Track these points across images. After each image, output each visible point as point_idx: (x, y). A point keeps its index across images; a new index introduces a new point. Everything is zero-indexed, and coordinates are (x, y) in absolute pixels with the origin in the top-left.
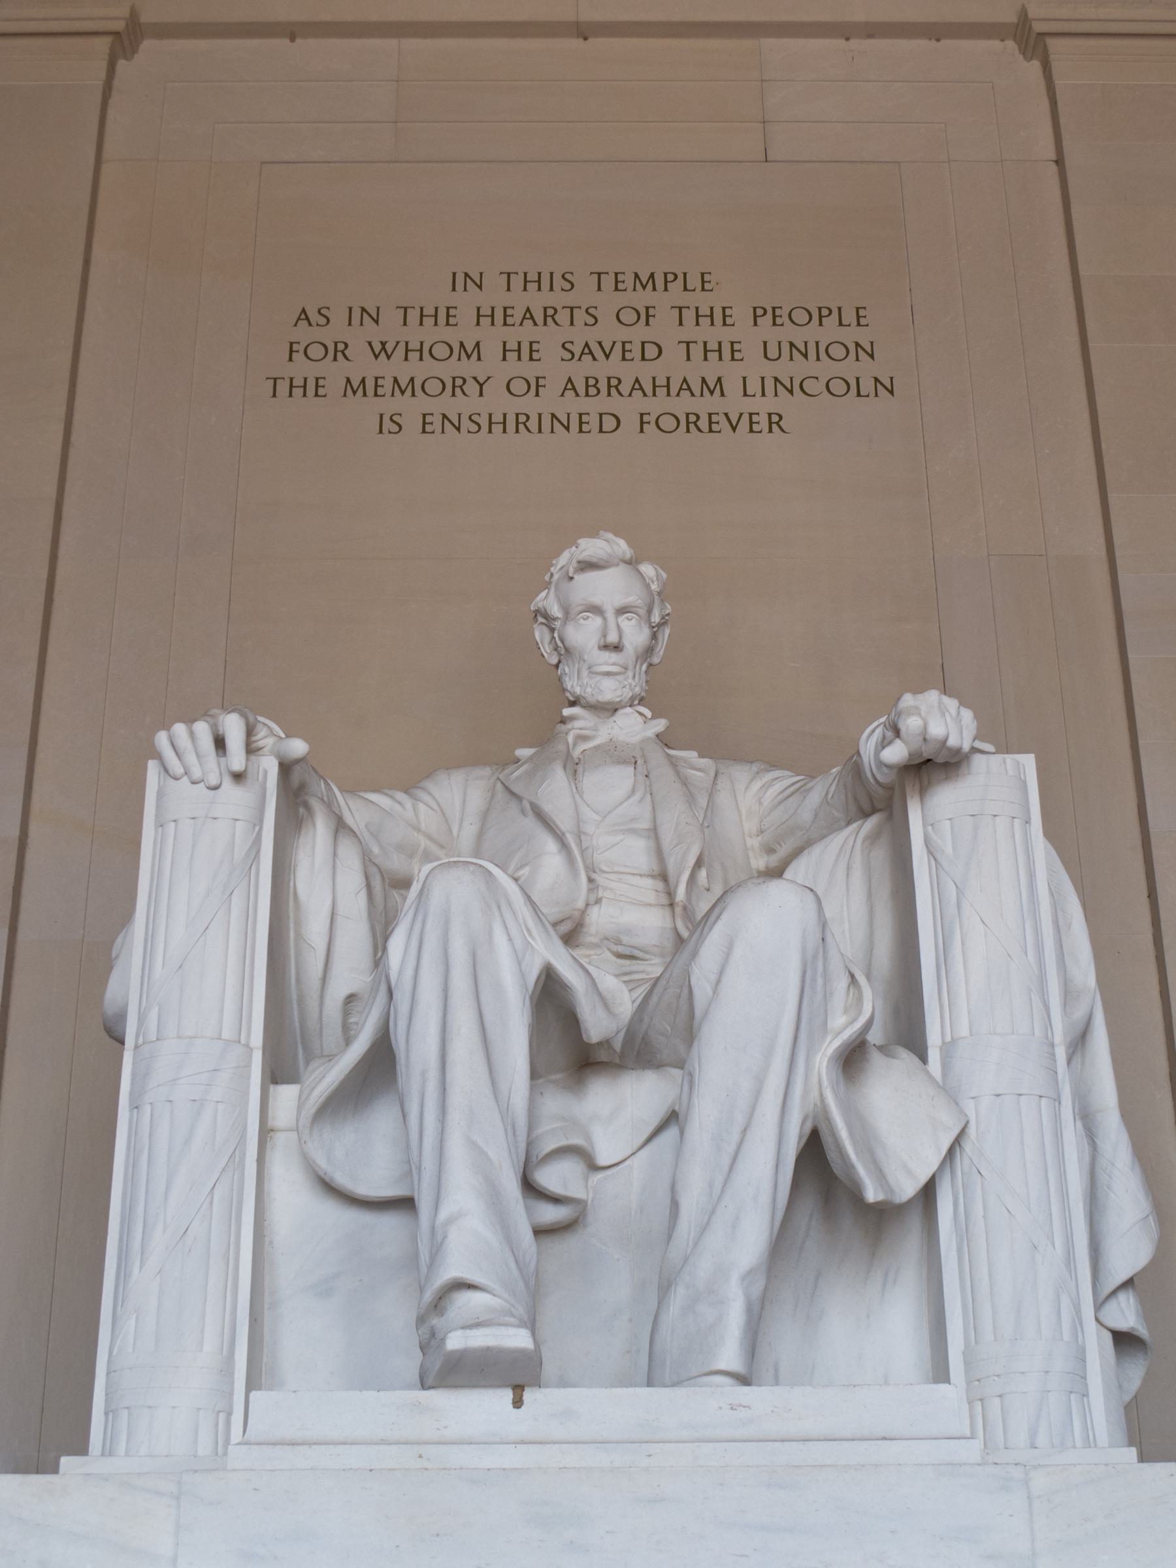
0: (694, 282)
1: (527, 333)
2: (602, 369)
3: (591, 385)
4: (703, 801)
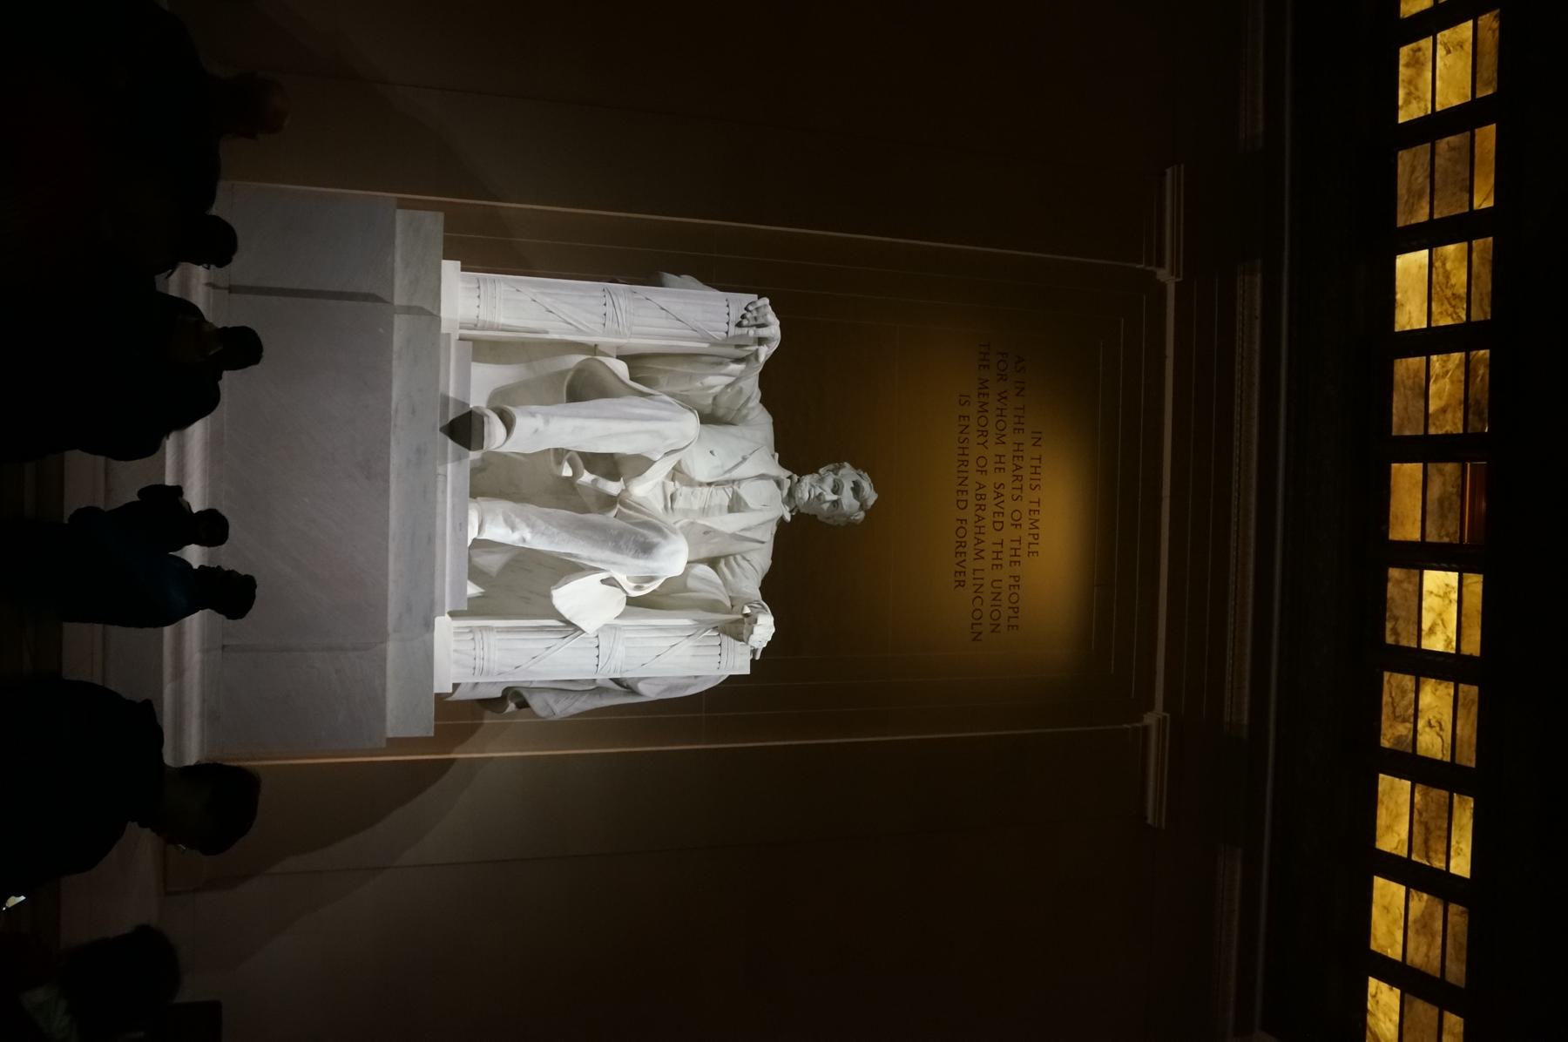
0: (1034, 548)
1: (1010, 467)
2: (990, 502)
3: (982, 497)
4: (748, 534)
